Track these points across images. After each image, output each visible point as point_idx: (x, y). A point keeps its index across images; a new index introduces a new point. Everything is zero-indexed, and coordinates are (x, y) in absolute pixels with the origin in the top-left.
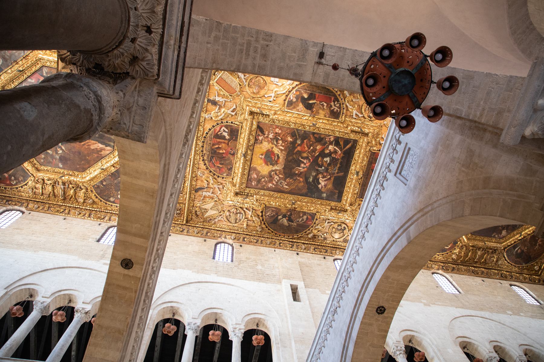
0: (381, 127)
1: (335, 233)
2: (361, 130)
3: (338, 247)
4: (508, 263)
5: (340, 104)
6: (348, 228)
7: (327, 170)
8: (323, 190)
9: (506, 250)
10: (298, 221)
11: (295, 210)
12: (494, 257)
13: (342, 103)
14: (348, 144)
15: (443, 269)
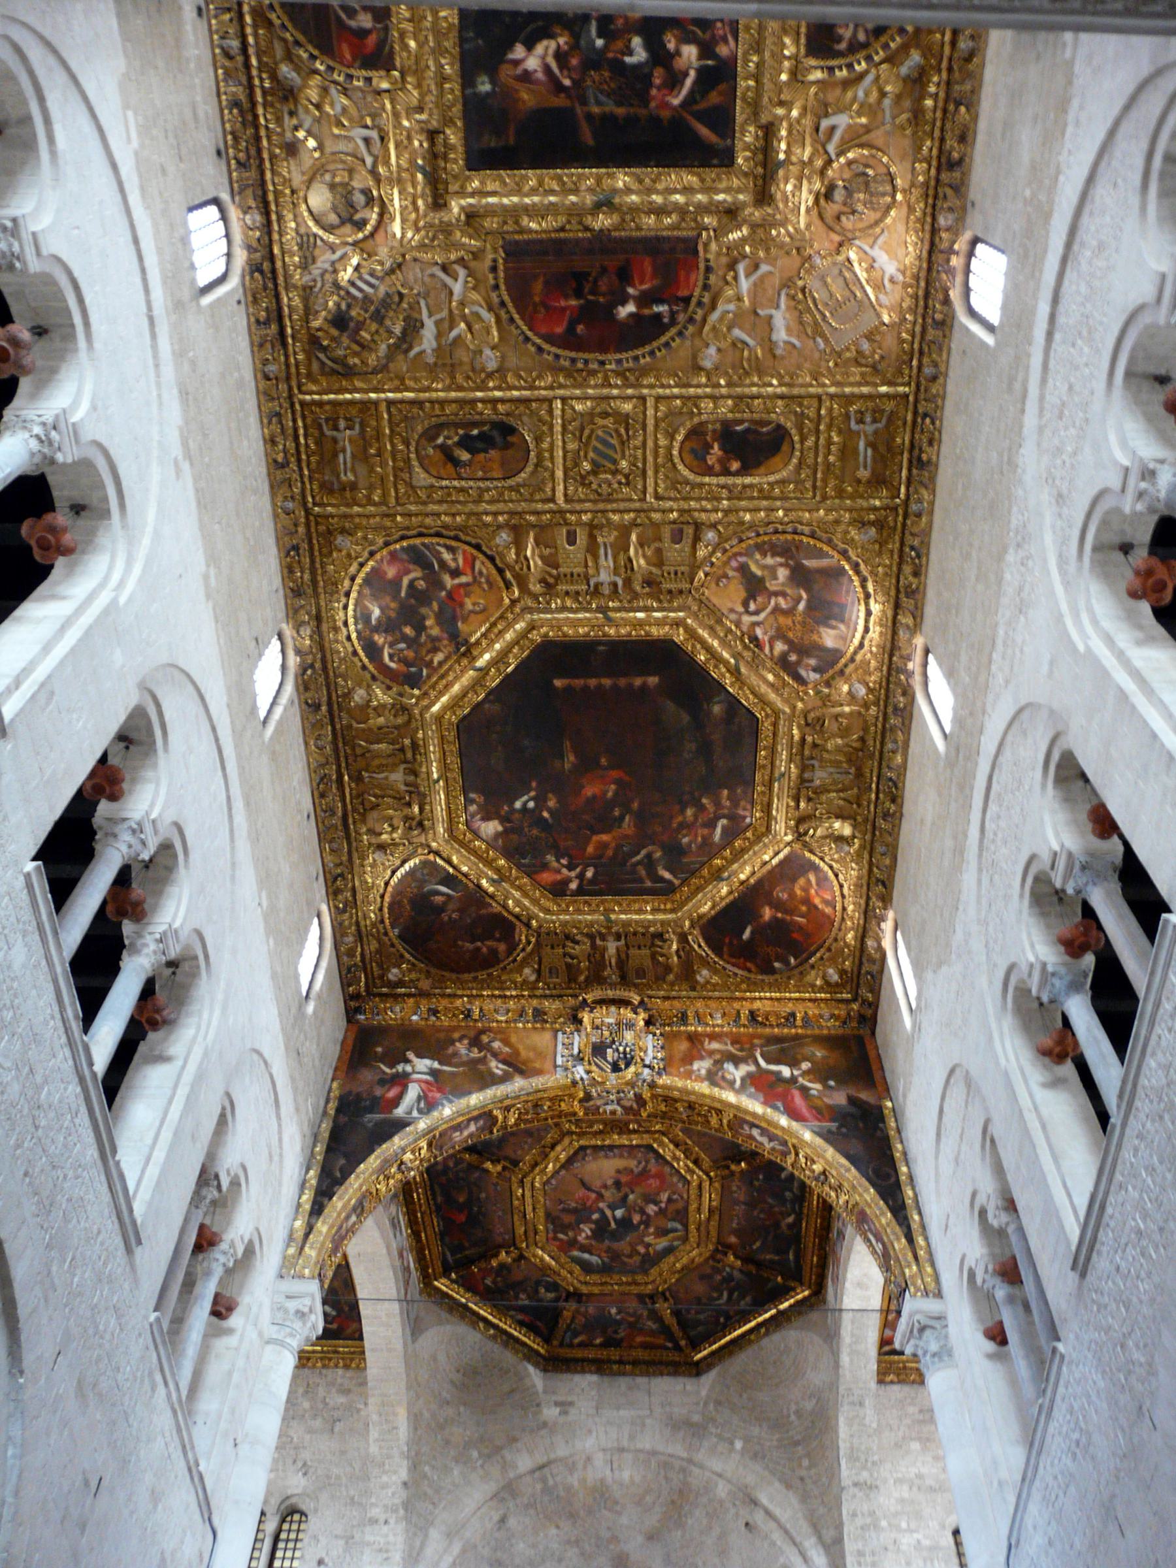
1: (332, 187)
2: (781, 164)
3: (274, 217)
5: (865, 46)
6: (366, 238)
7: (594, 61)
8: (506, 72)
9: (431, 857)
12: (394, 829)
13: (871, 51)
14: (712, 127)
15: (305, 671)
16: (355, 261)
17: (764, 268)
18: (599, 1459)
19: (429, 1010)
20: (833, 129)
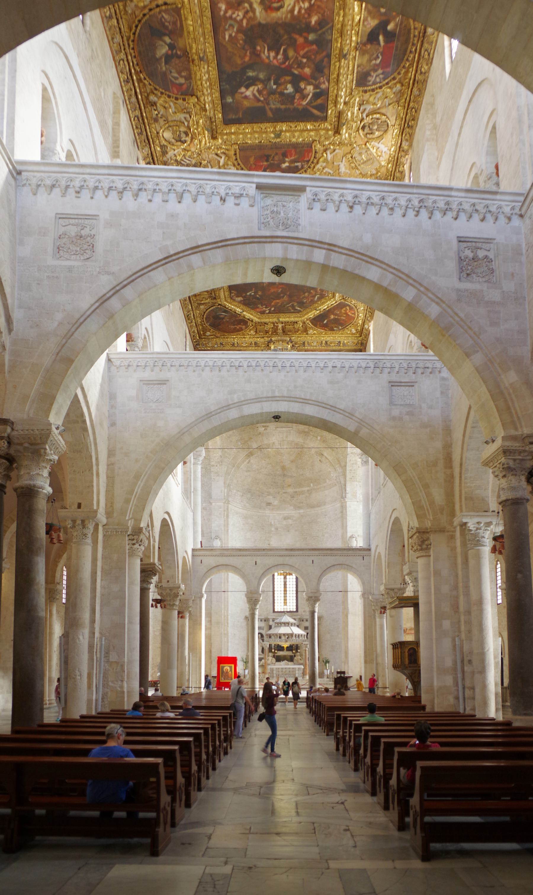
0: (350, 145)
5: (380, 83)
10: (171, 72)
11: (189, 62)
16: (183, 153)
17: (337, 151)
20: (365, 110)
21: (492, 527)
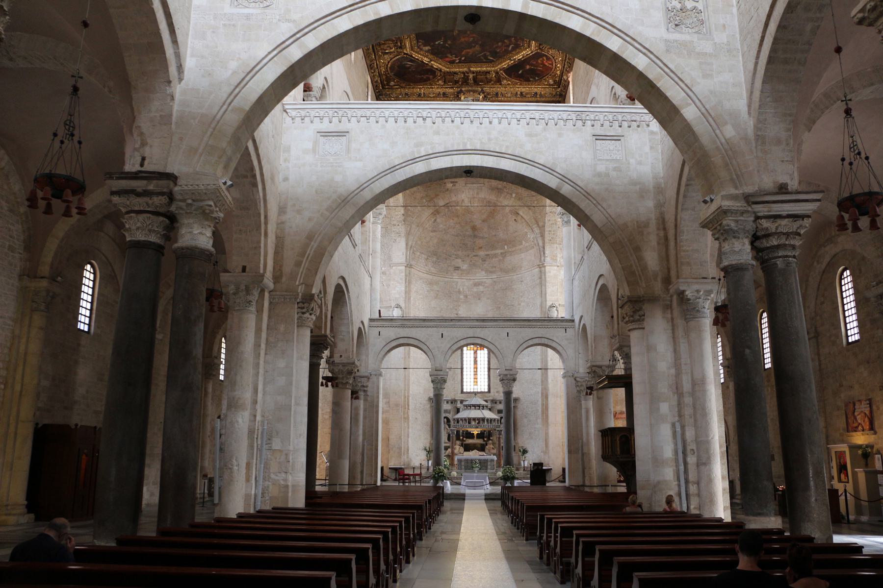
4: (389, 62)
12: (391, 48)
18: (466, 200)
19: (405, 94)
21: (712, 295)
